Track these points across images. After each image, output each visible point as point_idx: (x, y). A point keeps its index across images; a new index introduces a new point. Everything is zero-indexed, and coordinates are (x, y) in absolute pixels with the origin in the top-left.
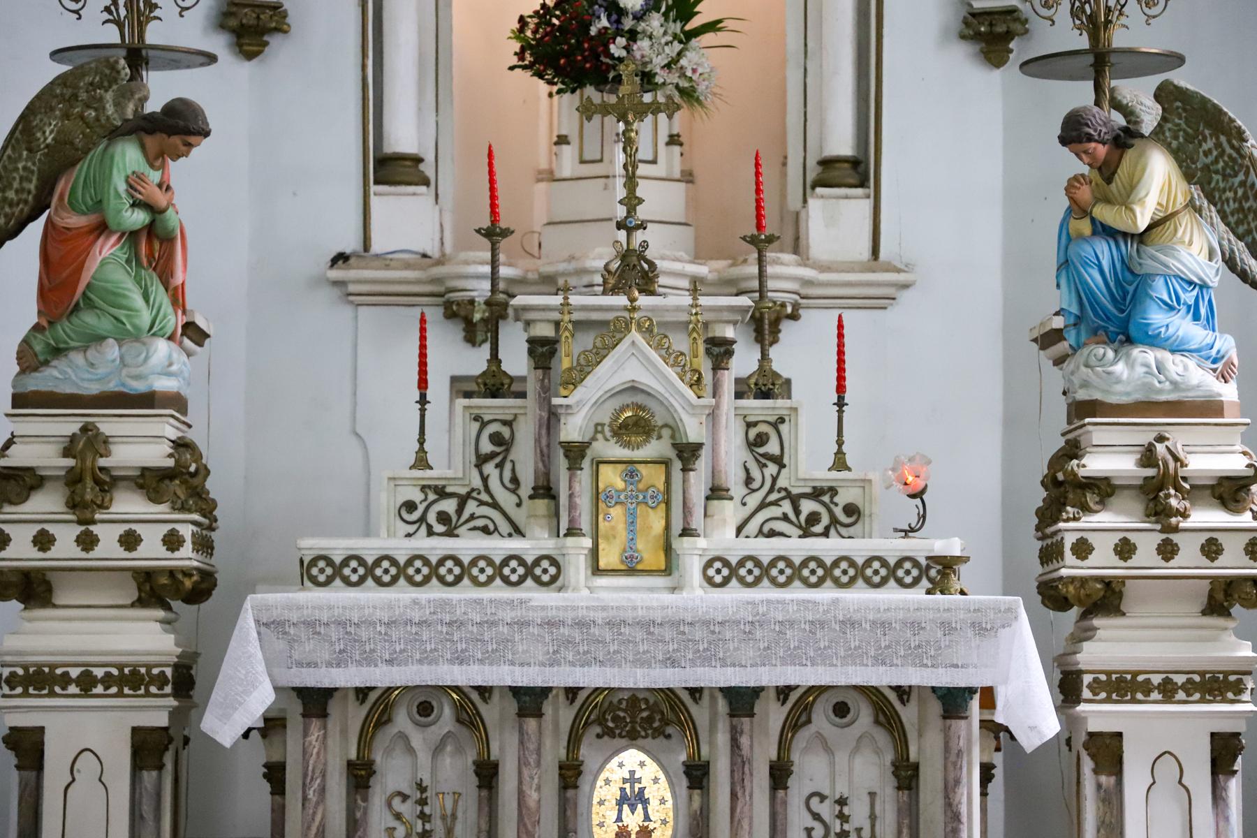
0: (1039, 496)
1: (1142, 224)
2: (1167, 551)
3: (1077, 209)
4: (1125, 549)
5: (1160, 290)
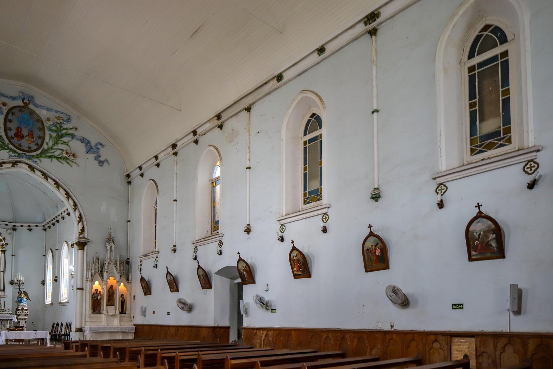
0: (16, 310)
1: (22, 297)
2: (23, 313)
3: (18, 296)
4: (21, 313)
5: (23, 300)
